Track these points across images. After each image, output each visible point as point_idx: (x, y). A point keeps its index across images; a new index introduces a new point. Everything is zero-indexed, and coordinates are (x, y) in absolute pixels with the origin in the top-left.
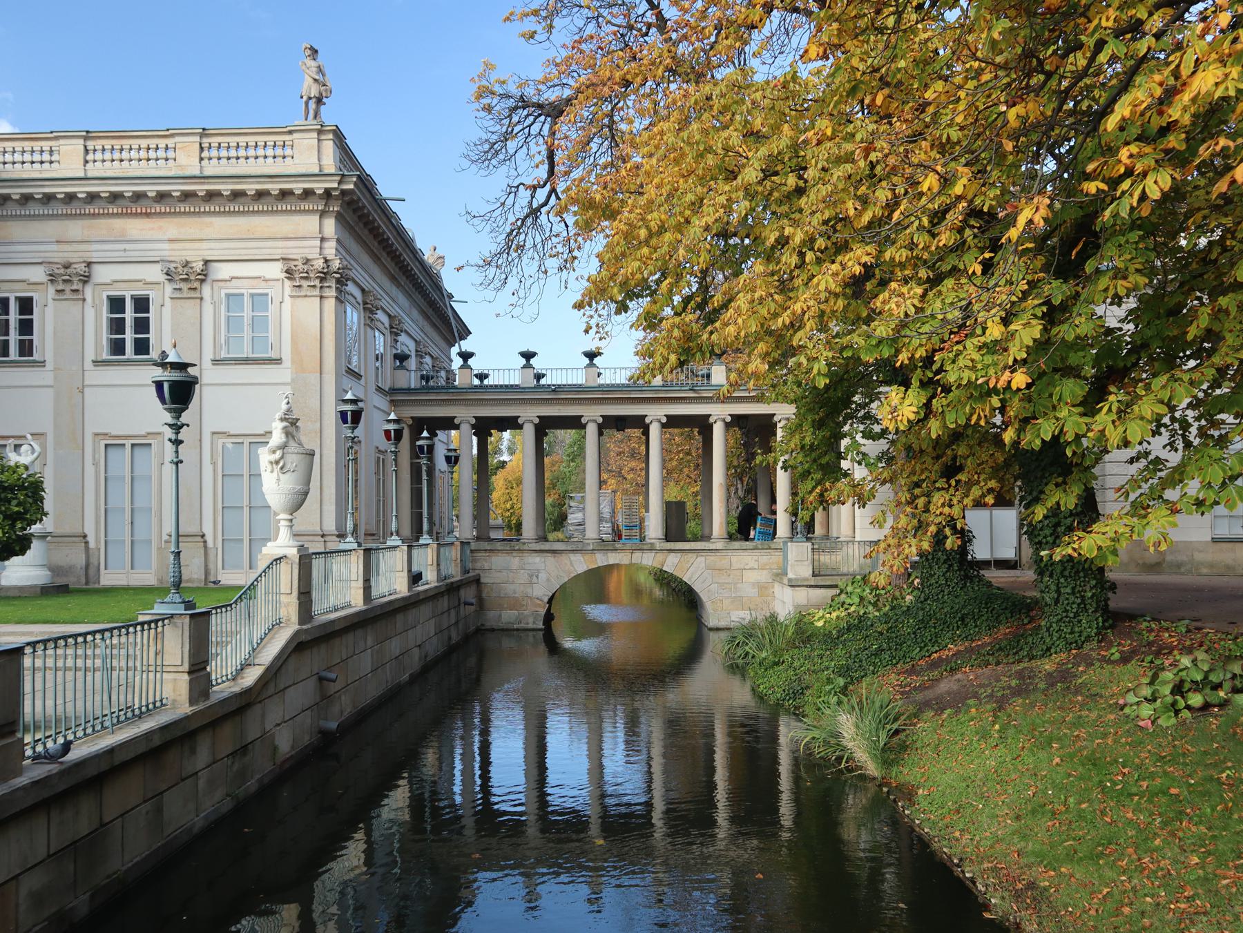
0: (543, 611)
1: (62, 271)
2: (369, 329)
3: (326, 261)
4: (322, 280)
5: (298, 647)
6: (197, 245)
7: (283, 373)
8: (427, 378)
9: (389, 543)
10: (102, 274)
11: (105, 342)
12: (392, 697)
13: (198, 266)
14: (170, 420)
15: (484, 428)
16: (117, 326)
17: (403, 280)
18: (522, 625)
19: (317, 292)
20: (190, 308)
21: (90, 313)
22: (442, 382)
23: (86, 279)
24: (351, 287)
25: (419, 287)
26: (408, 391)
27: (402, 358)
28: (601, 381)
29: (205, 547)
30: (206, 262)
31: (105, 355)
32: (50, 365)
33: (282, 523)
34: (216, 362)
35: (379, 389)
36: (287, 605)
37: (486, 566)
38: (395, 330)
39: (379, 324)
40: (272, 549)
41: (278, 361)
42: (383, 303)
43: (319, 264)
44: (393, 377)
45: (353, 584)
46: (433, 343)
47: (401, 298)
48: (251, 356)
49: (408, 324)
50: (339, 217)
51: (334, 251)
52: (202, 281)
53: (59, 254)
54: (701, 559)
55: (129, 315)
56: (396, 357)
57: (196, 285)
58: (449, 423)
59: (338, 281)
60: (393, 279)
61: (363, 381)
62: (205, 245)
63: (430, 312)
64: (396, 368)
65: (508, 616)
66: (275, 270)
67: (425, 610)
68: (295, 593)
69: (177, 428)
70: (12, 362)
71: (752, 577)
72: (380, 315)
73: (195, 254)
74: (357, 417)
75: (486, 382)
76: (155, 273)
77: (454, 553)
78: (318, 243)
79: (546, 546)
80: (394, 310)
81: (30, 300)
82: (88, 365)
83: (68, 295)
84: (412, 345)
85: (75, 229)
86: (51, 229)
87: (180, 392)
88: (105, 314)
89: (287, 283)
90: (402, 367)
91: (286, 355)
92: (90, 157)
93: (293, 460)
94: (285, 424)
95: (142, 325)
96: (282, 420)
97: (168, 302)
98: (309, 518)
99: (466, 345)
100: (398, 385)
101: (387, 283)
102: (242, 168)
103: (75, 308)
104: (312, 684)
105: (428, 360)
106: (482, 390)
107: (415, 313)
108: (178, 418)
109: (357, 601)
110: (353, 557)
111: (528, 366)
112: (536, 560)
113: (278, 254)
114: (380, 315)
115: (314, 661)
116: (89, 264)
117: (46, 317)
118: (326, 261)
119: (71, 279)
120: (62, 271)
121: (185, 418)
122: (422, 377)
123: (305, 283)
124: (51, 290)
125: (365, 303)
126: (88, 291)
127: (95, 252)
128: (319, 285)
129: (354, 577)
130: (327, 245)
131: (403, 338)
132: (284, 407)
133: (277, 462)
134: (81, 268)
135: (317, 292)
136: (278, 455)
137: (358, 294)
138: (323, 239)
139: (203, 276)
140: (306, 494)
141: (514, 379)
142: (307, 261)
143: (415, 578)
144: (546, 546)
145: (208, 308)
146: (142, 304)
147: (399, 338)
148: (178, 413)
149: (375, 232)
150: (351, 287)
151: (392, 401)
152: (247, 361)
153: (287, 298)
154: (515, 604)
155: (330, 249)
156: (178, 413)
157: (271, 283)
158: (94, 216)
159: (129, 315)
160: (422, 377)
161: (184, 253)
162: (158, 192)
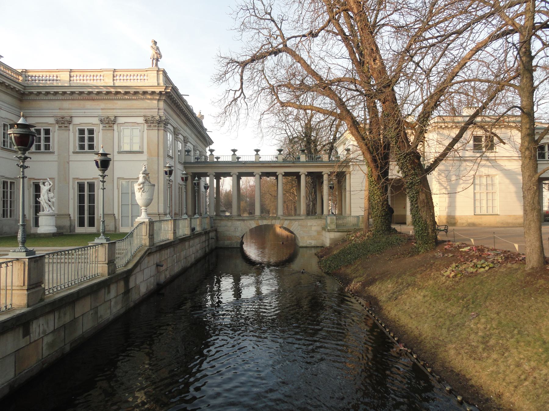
0: (239, 241)
1: (61, 119)
3: (160, 117)
4: (158, 123)
5: (149, 253)
6: (112, 111)
7: (144, 157)
8: (197, 159)
9: (183, 217)
10: (76, 121)
11: (77, 145)
12: (184, 271)
13: (112, 118)
14: (101, 174)
15: (218, 176)
16: (82, 139)
17: (188, 124)
18: (232, 246)
19: (157, 128)
20: (109, 133)
21: (71, 135)
22: (203, 160)
23: (70, 122)
24: (169, 126)
25: (194, 126)
26: (191, 163)
27: (188, 151)
28: (261, 160)
29: (115, 219)
30: (115, 117)
32: (56, 153)
33: (143, 210)
34: (119, 152)
35: (179, 162)
36: (145, 239)
37: (219, 225)
38: (186, 141)
39: (180, 140)
40: (139, 220)
41: (142, 152)
42: (181, 132)
43: (158, 118)
44: (185, 158)
45: (170, 232)
46: (200, 145)
47: (188, 131)
49: (191, 139)
50: (165, 101)
52: (114, 123)
53: (60, 113)
54: (297, 222)
55: (86, 135)
56: (186, 151)
57: (111, 125)
58: (205, 175)
59: (165, 124)
60: (185, 123)
61: (173, 160)
62: (115, 111)
63: (199, 135)
65: (227, 243)
66: (141, 120)
67: (197, 240)
68: (148, 235)
69: (104, 177)
71: (314, 228)
72: (180, 136)
73: (111, 114)
74: (171, 173)
75: (219, 160)
76: (96, 121)
77: (207, 221)
78: (157, 110)
79: (241, 218)
80: (186, 134)
81: (49, 130)
82: (71, 153)
83: (63, 128)
84: (192, 147)
85: (66, 104)
86: (57, 104)
87: (104, 164)
89: (146, 125)
90: (188, 155)
91: (145, 150)
95: (91, 139)
96: (143, 174)
97: (101, 131)
98: (153, 209)
99: (212, 147)
100: (188, 161)
101: (183, 125)
103: (66, 133)
104: (154, 267)
105: (198, 152)
106: (218, 163)
107: (193, 136)
108: (103, 173)
109: (170, 236)
110: (170, 223)
111: (234, 154)
112: (238, 223)
113: (142, 114)
114: (180, 136)
115: (155, 258)
116: (71, 117)
117: (56, 136)
118: (160, 117)
119: (64, 122)
120: (61, 119)
121: (106, 173)
123: (152, 125)
124: (57, 126)
125: (174, 132)
126: (71, 127)
127: (73, 113)
128: (157, 125)
129: (170, 229)
130: (160, 111)
131: (189, 144)
132: (144, 169)
133: (141, 189)
134: (68, 119)
135: (157, 128)
136: (141, 186)
137: (172, 128)
138: (159, 109)
139: (114, 122)
140: (152, 200)
141: (229, 159)
143: (193, 229)
144: (241, 218)
146: (91, 132)
148: (104, 171)
149: (178, 106)
150: (169, 126)
151: (185, 168)
153: (145, 130)
154: (230, 238)
155: (162, 113)
156: (104, 171)
158: (73, 100)
159: (86, 135)
160: (196, 158)
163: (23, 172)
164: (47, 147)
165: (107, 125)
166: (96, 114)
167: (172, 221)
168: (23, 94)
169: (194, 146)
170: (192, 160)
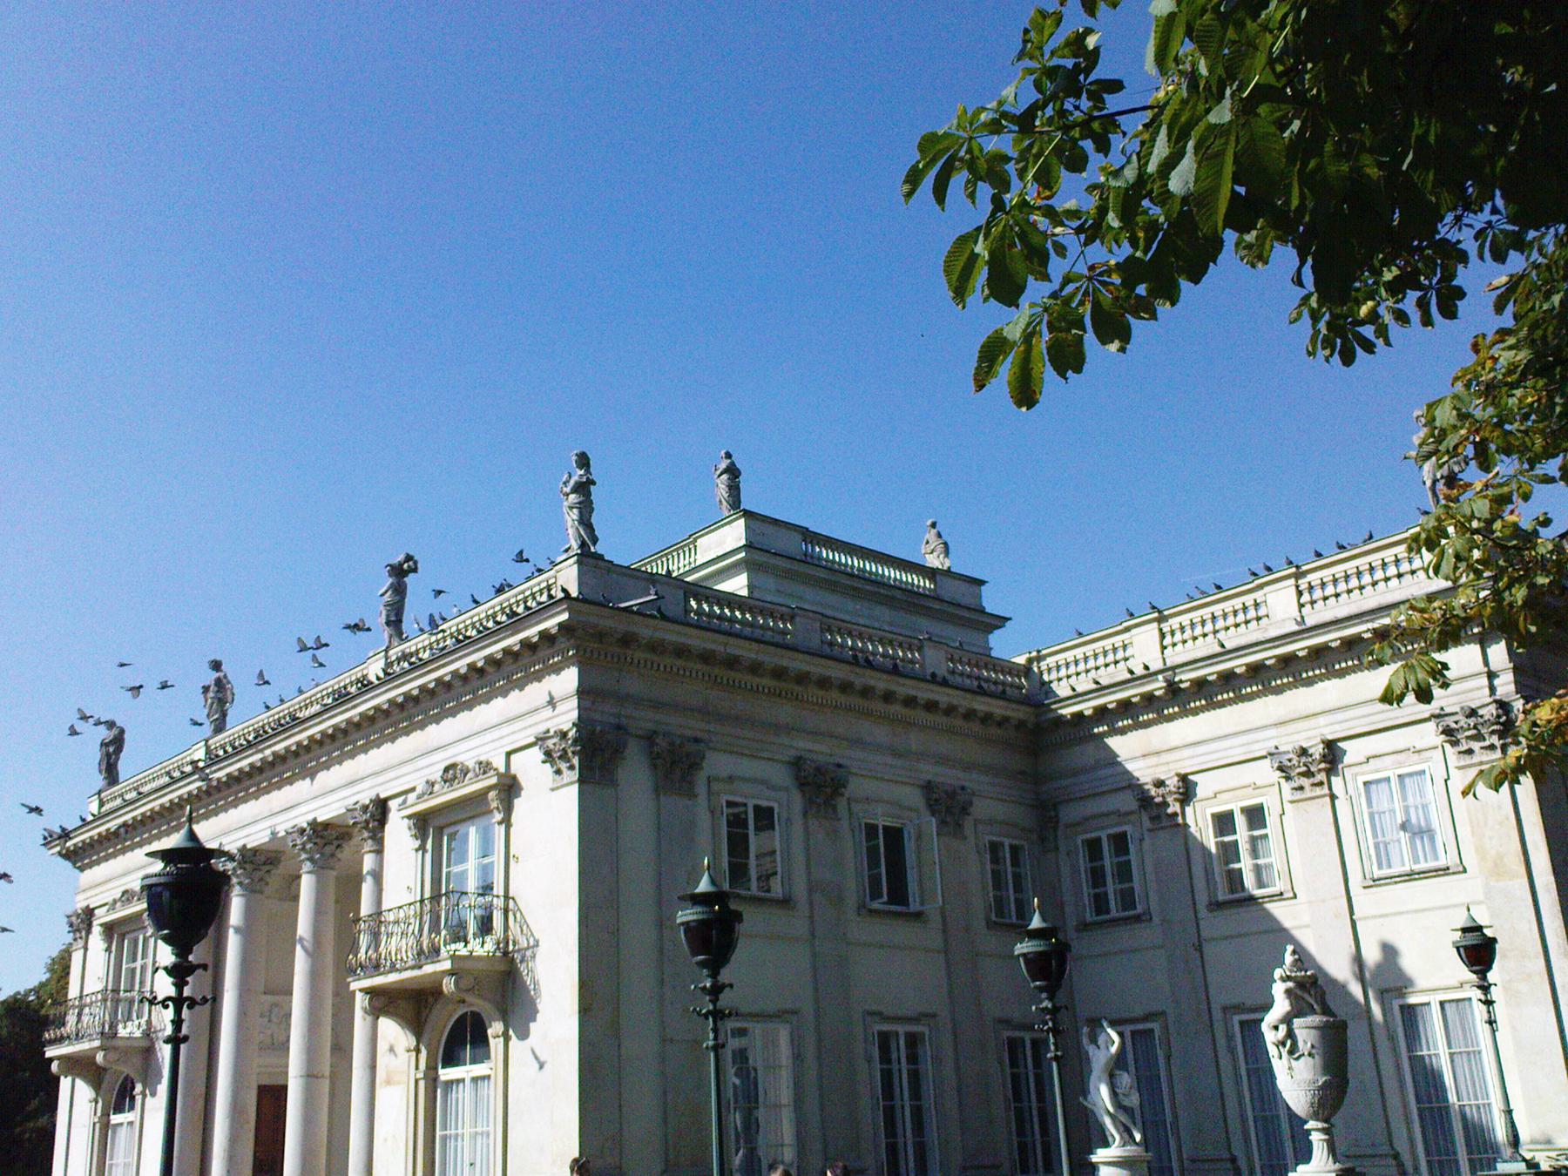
43: (1490, 712)
48: (1417, 868)
51: (1512, 687)
62: (1322, 720)
70: (1113, 920)
73: (1312, 736)
78: (1484, 681)
92: (1306, 598)
94: (1290, 984)
102: (1371, 599)
128: (1498, 743)
142: (1473, 713)
152: (1410, 876)
157: (1427, 754)
161: (1296, 737)
162: (1247, 665)
164: (1128, 899)
165: (1305, 782)
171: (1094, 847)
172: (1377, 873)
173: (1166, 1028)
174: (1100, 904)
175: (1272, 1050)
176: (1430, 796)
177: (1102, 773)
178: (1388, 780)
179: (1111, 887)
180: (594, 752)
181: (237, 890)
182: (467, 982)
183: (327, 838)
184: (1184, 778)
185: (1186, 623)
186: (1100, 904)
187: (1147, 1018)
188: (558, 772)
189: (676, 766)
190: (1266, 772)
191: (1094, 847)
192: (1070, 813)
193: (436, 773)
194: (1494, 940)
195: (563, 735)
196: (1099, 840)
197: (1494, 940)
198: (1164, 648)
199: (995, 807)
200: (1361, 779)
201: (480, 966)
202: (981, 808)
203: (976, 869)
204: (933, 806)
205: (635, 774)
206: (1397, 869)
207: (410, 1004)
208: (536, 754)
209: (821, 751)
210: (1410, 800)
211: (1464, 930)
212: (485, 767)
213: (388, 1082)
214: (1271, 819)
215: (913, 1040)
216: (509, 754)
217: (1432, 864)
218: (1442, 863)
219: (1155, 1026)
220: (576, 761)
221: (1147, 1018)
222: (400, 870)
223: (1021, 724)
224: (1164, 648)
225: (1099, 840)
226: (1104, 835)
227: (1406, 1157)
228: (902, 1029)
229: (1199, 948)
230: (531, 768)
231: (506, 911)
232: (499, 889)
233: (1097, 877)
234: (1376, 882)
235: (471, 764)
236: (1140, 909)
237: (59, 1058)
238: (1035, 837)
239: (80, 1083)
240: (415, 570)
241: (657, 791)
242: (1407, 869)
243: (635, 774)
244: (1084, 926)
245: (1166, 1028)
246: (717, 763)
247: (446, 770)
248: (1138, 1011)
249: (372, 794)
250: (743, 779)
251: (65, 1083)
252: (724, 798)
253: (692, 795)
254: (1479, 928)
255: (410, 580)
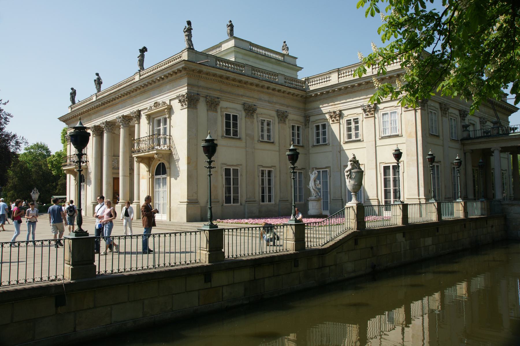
2: (444, 119)
31: (346, 140)
57: (373, 112)
64: (464, 131)
83: (336, 122)
84: (477, 120)
88: (346, 126)
93: (354, 175)
96: (351, 161)
114: (451, 110)
122: (484, 132)
125: (441, 108)
131: (469, 117)
136: (348, 173)
145: (377, 120)
147: (466, 119)
151: (462, 144)
152: (390, 137)
153: (403, 112)
160: (484, 132)
163: (210, 171)
164: (324, 140)
166: (359, 105)
167: (401, 206)
168: (306, 98)
169: (480, 118)
170: (479, 134)
171: (318, 127)
172: (383, 135)
173: (330, 171)
174: (318, 141)
175: (346, 177)
176: (397, 118)
177: (317, 110)
178: (387, 114)
179: (321, 137)
180: (191, 101)
181: (105, 132)
182: (160, 156)
183: (127, 119)
184: (340, 111)
185: (345, 72)
186: (318, 141)
187: (326, 168)
188: (182, 105)
189: (213, 104)
190: (360, 111)
191: (318, 127)
192: (312, 119)
193: (152, 104)
194: (402, 153)
195: (183, 96)
196: (319, 126)
197: (402, 153)
198: (339, 78)
199: (294, 117)
200: (382, 113)
201: (163, 152)
202: (291, 117)
203: (288, 132)
204: (278, 116)
205: (202, 106)
206: (387, 135)
207: (148, 161)
208: (177, 101)
209: (250, 101)
210: (392, 119)
211: (396, 150)
212: (164, 103)
213: (143, 178)
214: (360, 122)
215: (269, 172)
216: (170, 100)
217: (395, 134)
218: (397, 134)
219: (328, 170)
220: (187, 103)
221: (326, 168)
222: (144, 129)
223: (302, 96)
224: (339, 78)
225: (319, 126)
226: (320, 124)
227: (380, 200)
228: (267, 169)
229: (340, 152)
230: (176, 105)
231: (170, 139)
232: (168, 133)
233: (318, 134)
234: (383, 138)
235: (161, 102)
236: (327, 143)
237: (66, 170)
238: (303, 124)
239: (72, 176)
240: (147, 51)
241: (207, 110)
242: (389, 135)
243: (202, 106)
244: (314, 146)
245: (330, 171)
246: (223, 104)
247: (155, 104)
248: (324, 166)
249: (137, 109)
250: (230, 108)
251: (68, 175)
252: (225, 113)
253: (216, 112)
254: (399, 150)
255: (145, 53)
